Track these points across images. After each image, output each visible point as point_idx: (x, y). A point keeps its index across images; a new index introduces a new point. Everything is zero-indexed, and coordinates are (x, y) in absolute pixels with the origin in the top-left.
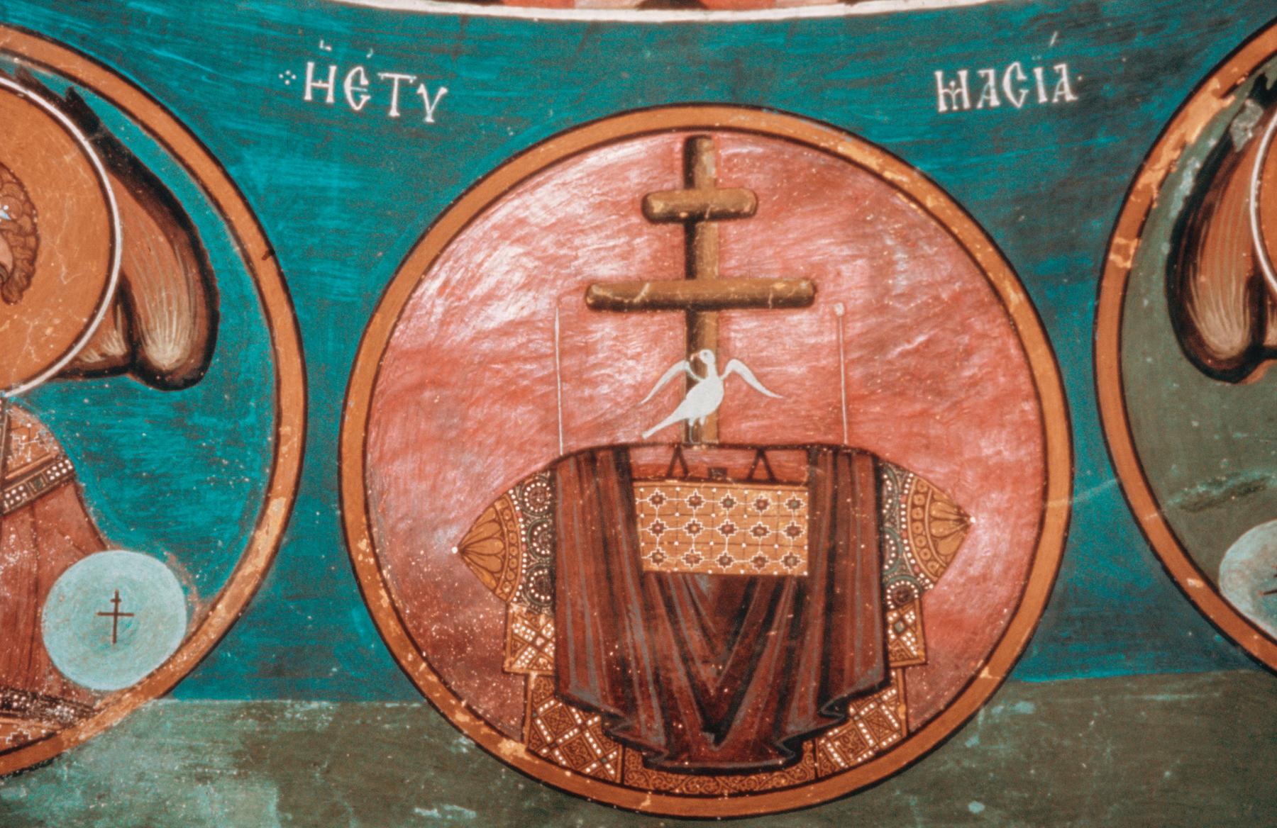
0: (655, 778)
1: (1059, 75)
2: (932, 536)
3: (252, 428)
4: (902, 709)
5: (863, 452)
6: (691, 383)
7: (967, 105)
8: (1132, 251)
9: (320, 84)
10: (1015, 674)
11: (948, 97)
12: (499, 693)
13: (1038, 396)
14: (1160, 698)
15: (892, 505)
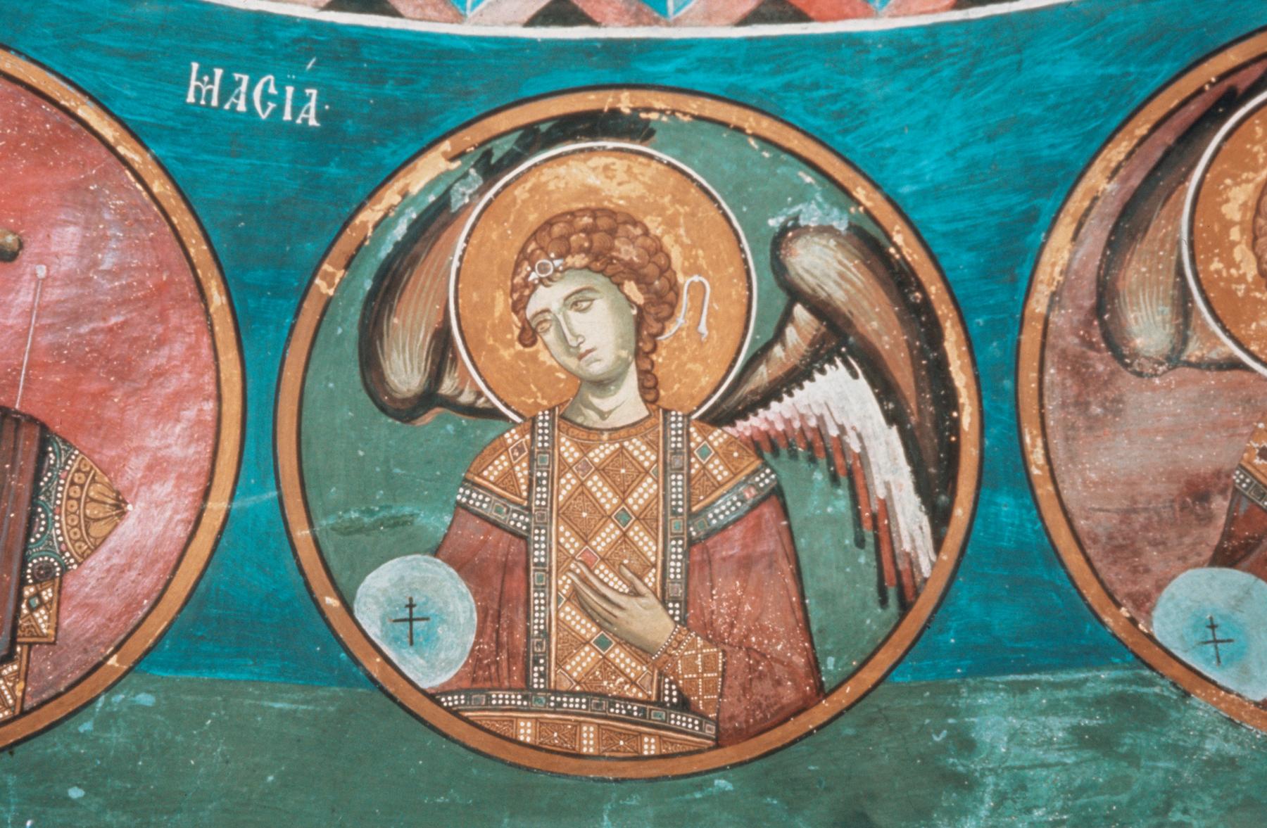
1: (308, 99)
2: (85, 516)
4: (21, 686)
5: (32, 420)
7: (214, 103)
8: (337, 280)
10: (143, 666)
11: (198, 90)
13: (219, 398)
14: (278, 705)
15: (50, 478)
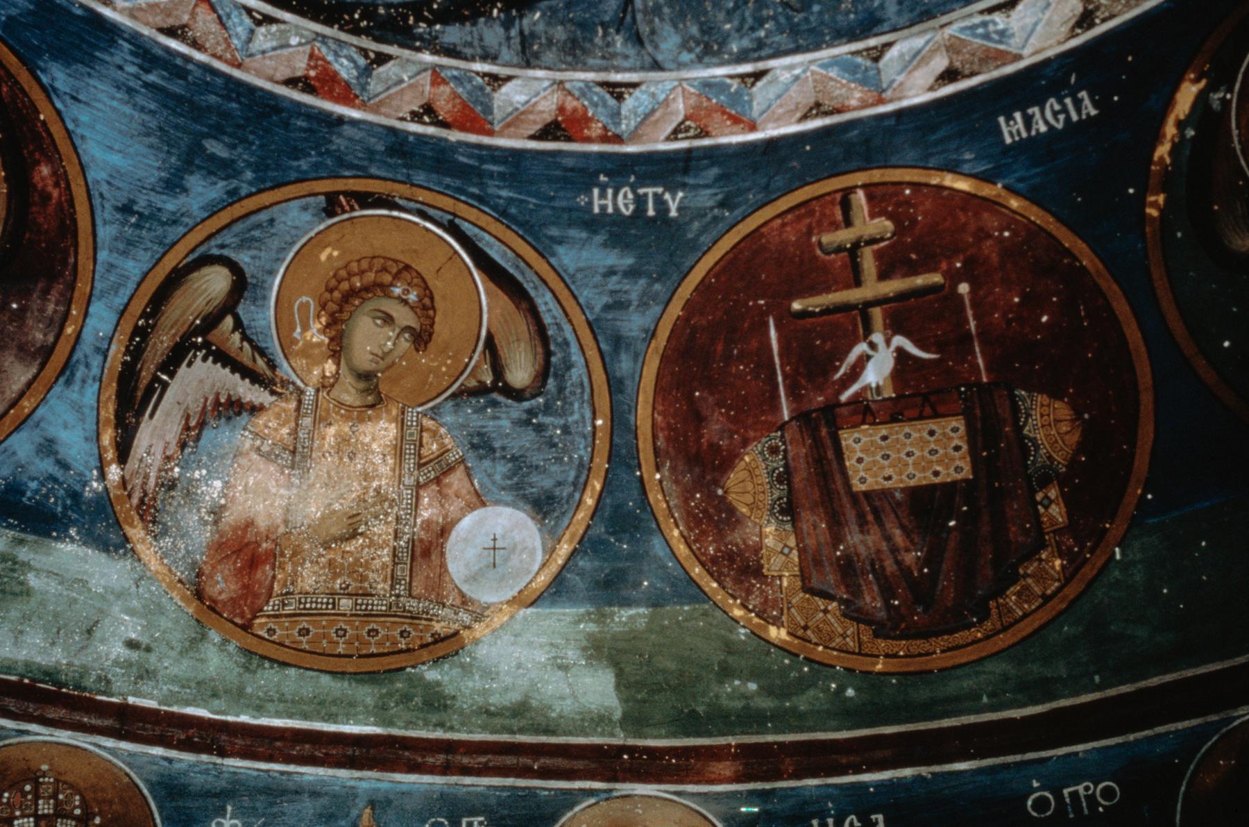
0: (882, 644)
1: (1082, 100)
3: (577, 422)
6: (869, 358)
7: (1024, 135)
9: (603, 202)
12: (762, 591)
